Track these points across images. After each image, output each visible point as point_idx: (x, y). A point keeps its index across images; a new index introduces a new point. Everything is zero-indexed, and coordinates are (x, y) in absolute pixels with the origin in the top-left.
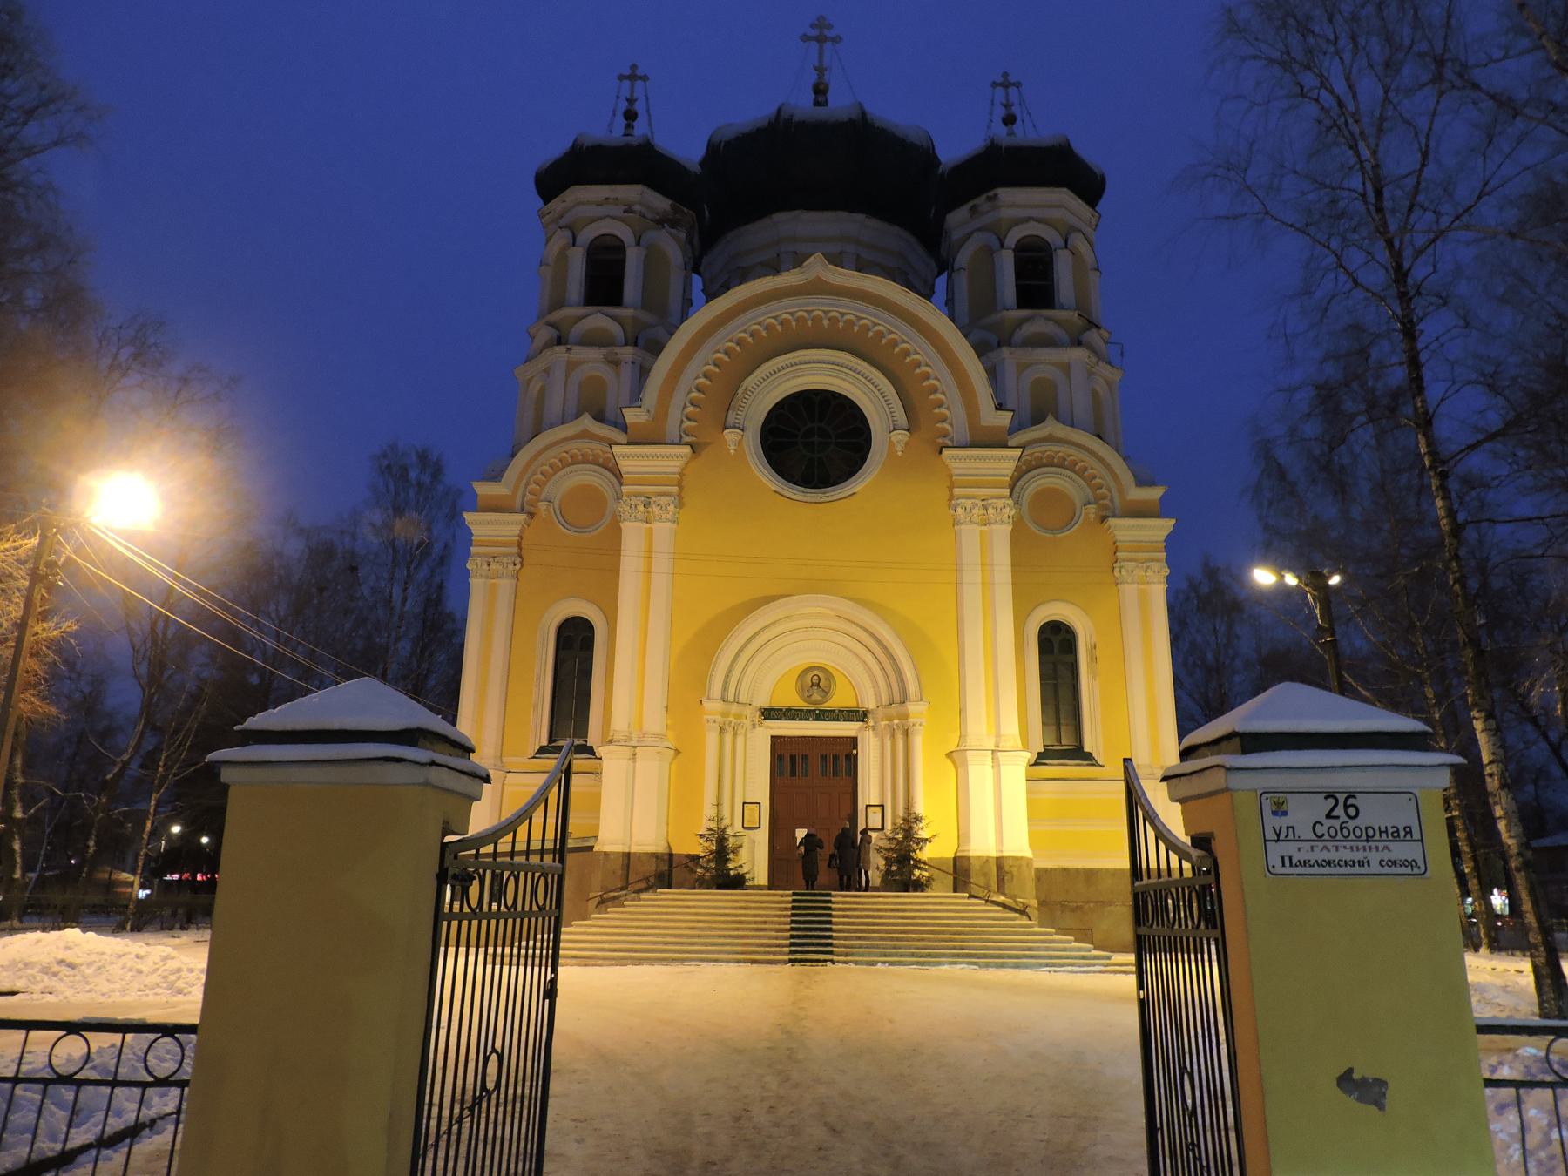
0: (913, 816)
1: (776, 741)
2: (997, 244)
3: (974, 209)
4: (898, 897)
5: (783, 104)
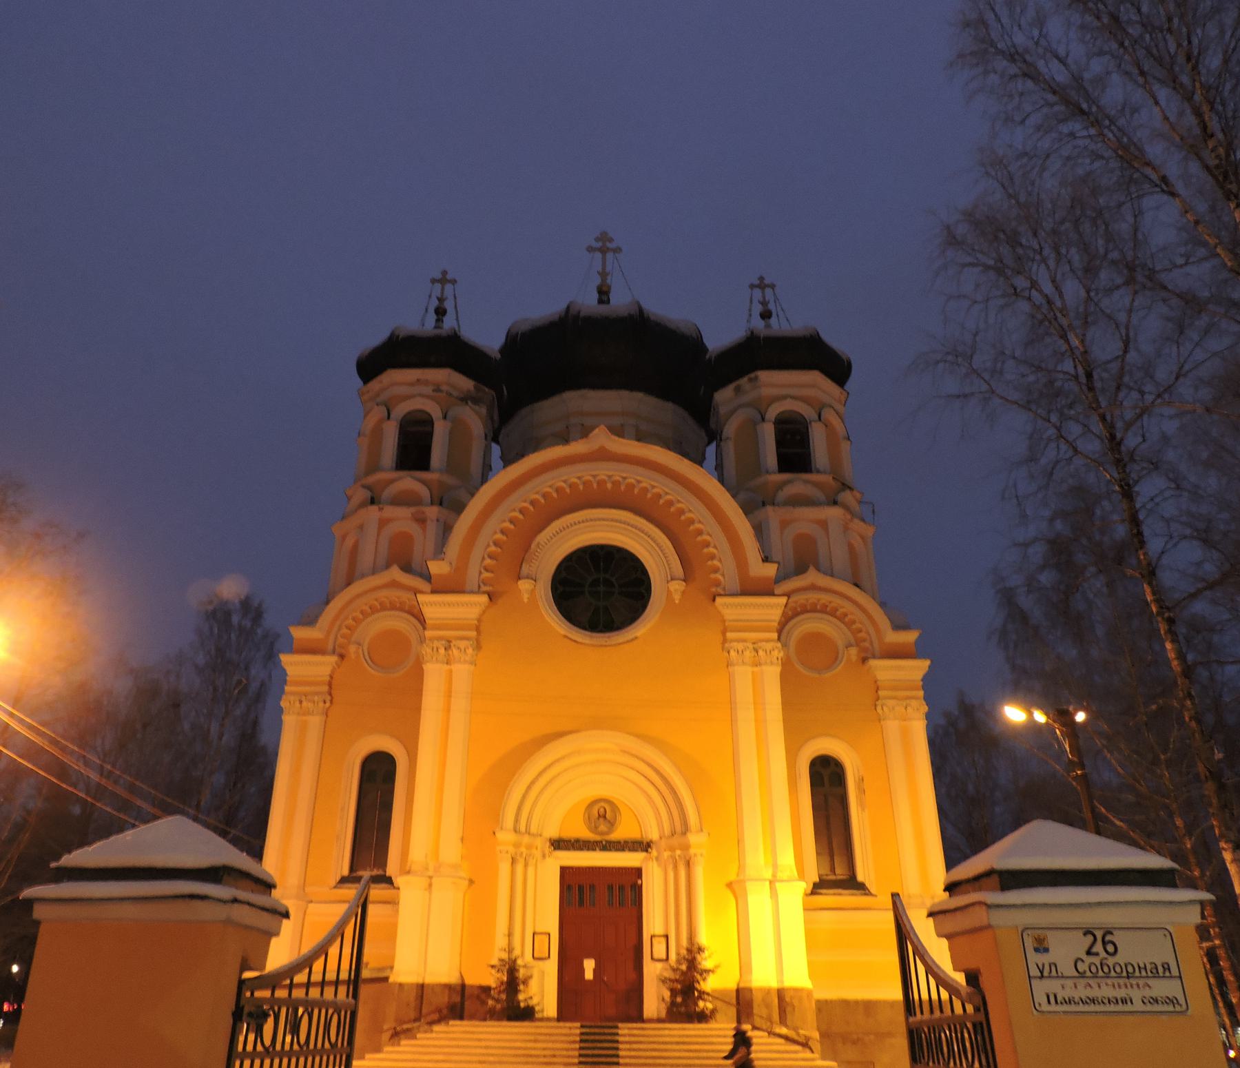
1: (564, 871)
3: (738, 390)
4: (684, 1029)
5: (571, 302)
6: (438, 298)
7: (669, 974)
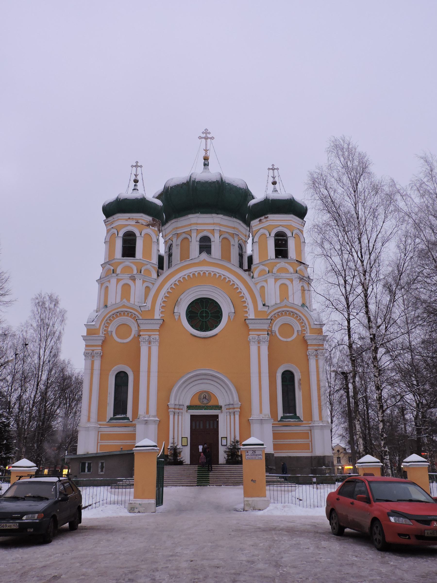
0: (236, 441)
2: (268, 235)
3: (260, 220)
4: (230, 466)
5: (192, 174)
6: (135, 175)
7: (227, 450)
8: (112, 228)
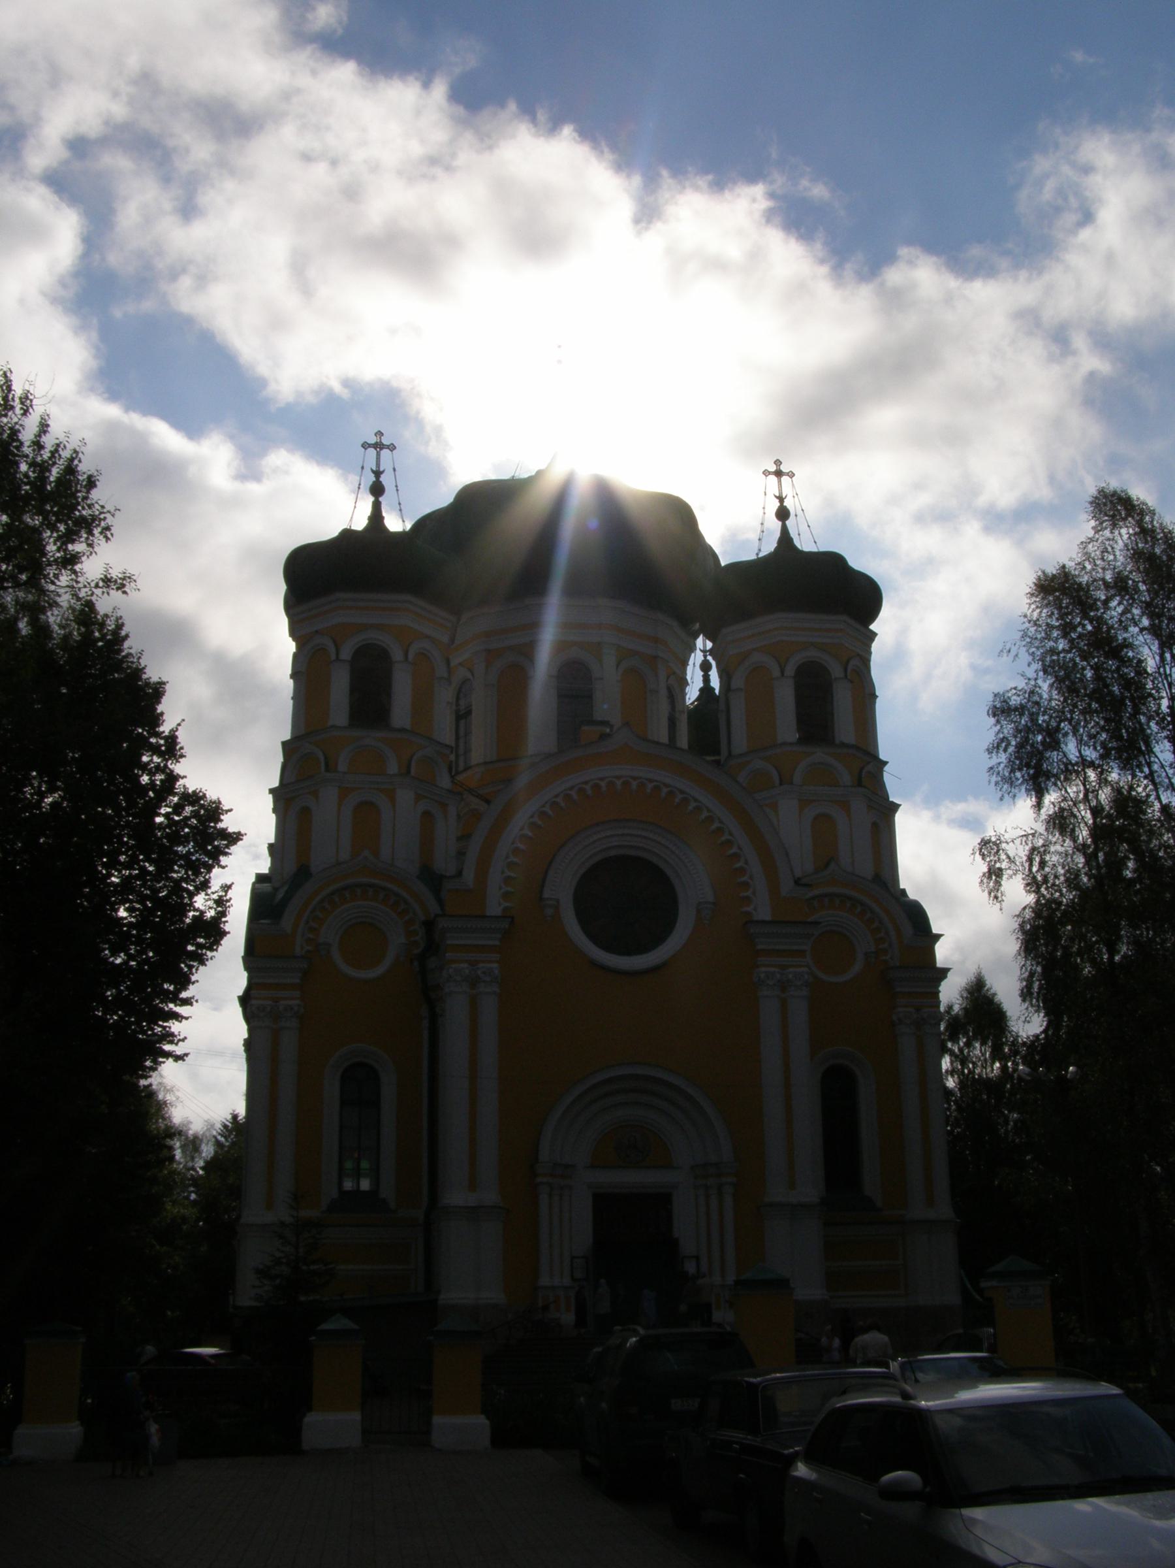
2: (776, 673)
6: (373, 471)
8: (317, 632)
